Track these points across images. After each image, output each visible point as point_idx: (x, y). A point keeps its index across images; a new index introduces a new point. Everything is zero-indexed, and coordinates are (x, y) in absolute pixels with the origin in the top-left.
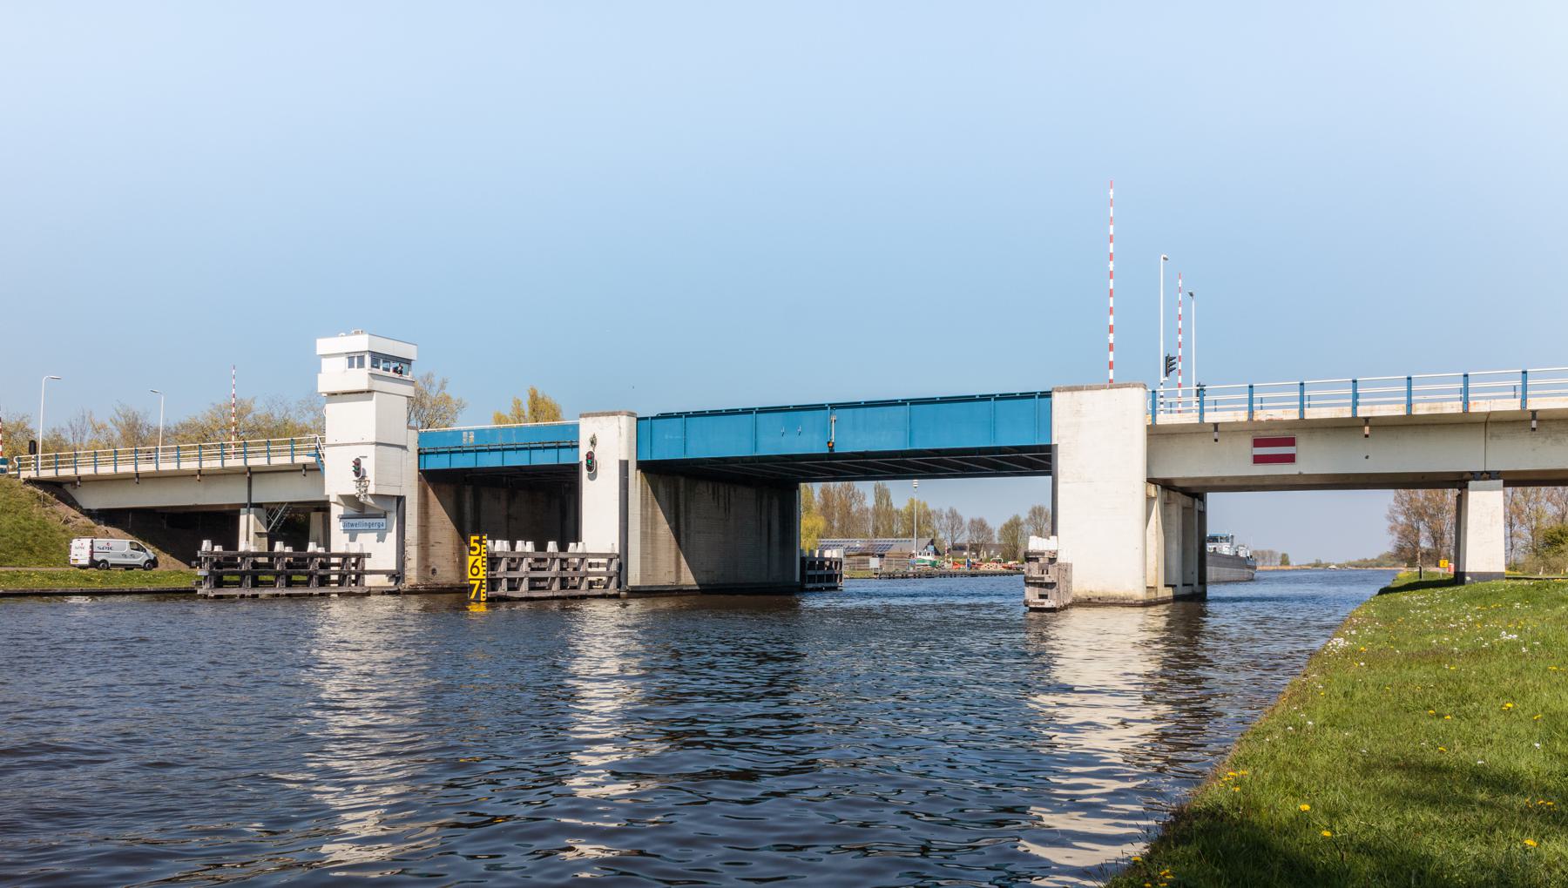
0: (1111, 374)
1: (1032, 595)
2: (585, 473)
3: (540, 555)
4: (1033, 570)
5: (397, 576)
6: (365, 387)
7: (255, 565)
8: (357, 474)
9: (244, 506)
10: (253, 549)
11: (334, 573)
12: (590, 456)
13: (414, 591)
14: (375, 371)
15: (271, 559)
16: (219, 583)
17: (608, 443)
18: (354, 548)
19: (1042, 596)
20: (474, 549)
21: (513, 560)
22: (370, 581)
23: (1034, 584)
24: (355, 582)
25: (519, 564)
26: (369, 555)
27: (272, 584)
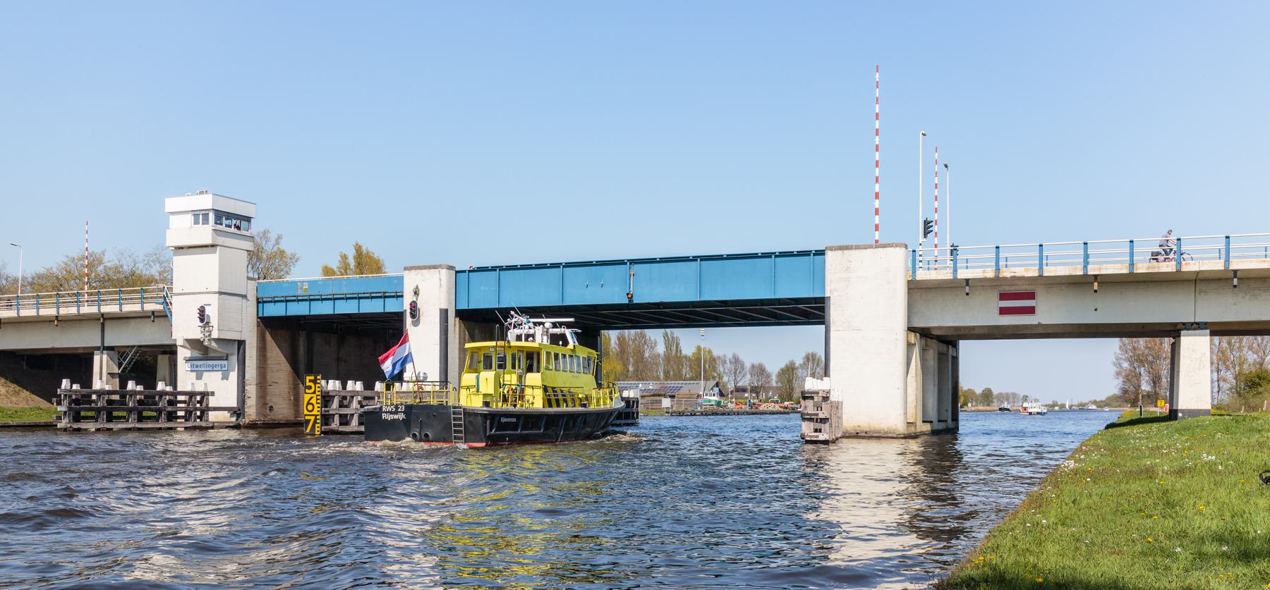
0: (877, 235)
1: (807, 429)
2: (409, 320)
3: (368, 393)
4: (809, 407)
5: (238, 412)
6: (209, 241)
7: (110, 402)
8: (202, 320)
9: (98, 348)
10: (107, 388)
11: (181, 409)
12: (414, 306)
13: (252, 426)
14: (219, 227)
15: (123, 396)
16: (77, 418)
18: (200, 387)
19: (816, 431)
20: (310, 388)
21: (344, 398)
22: (213, 416)
23: (810, 420)
24: (200, 418)
25: (351, 402)
26: (213, 394)
27: (126, 419)
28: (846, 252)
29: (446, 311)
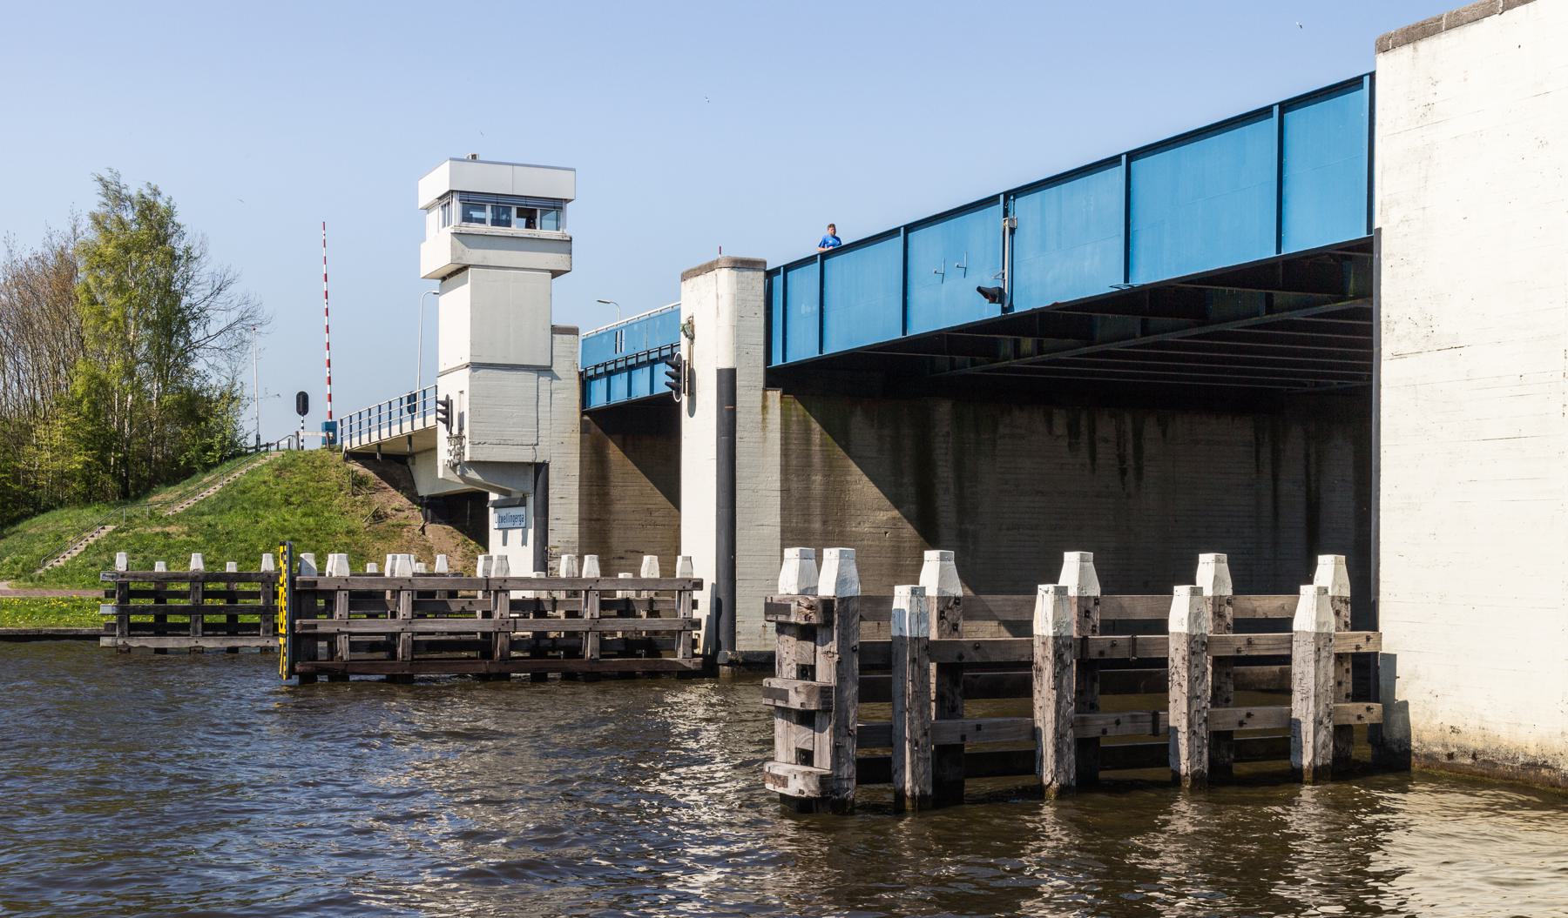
17: (716, 331)
28: (1425, 46)
29: (732, 373)
